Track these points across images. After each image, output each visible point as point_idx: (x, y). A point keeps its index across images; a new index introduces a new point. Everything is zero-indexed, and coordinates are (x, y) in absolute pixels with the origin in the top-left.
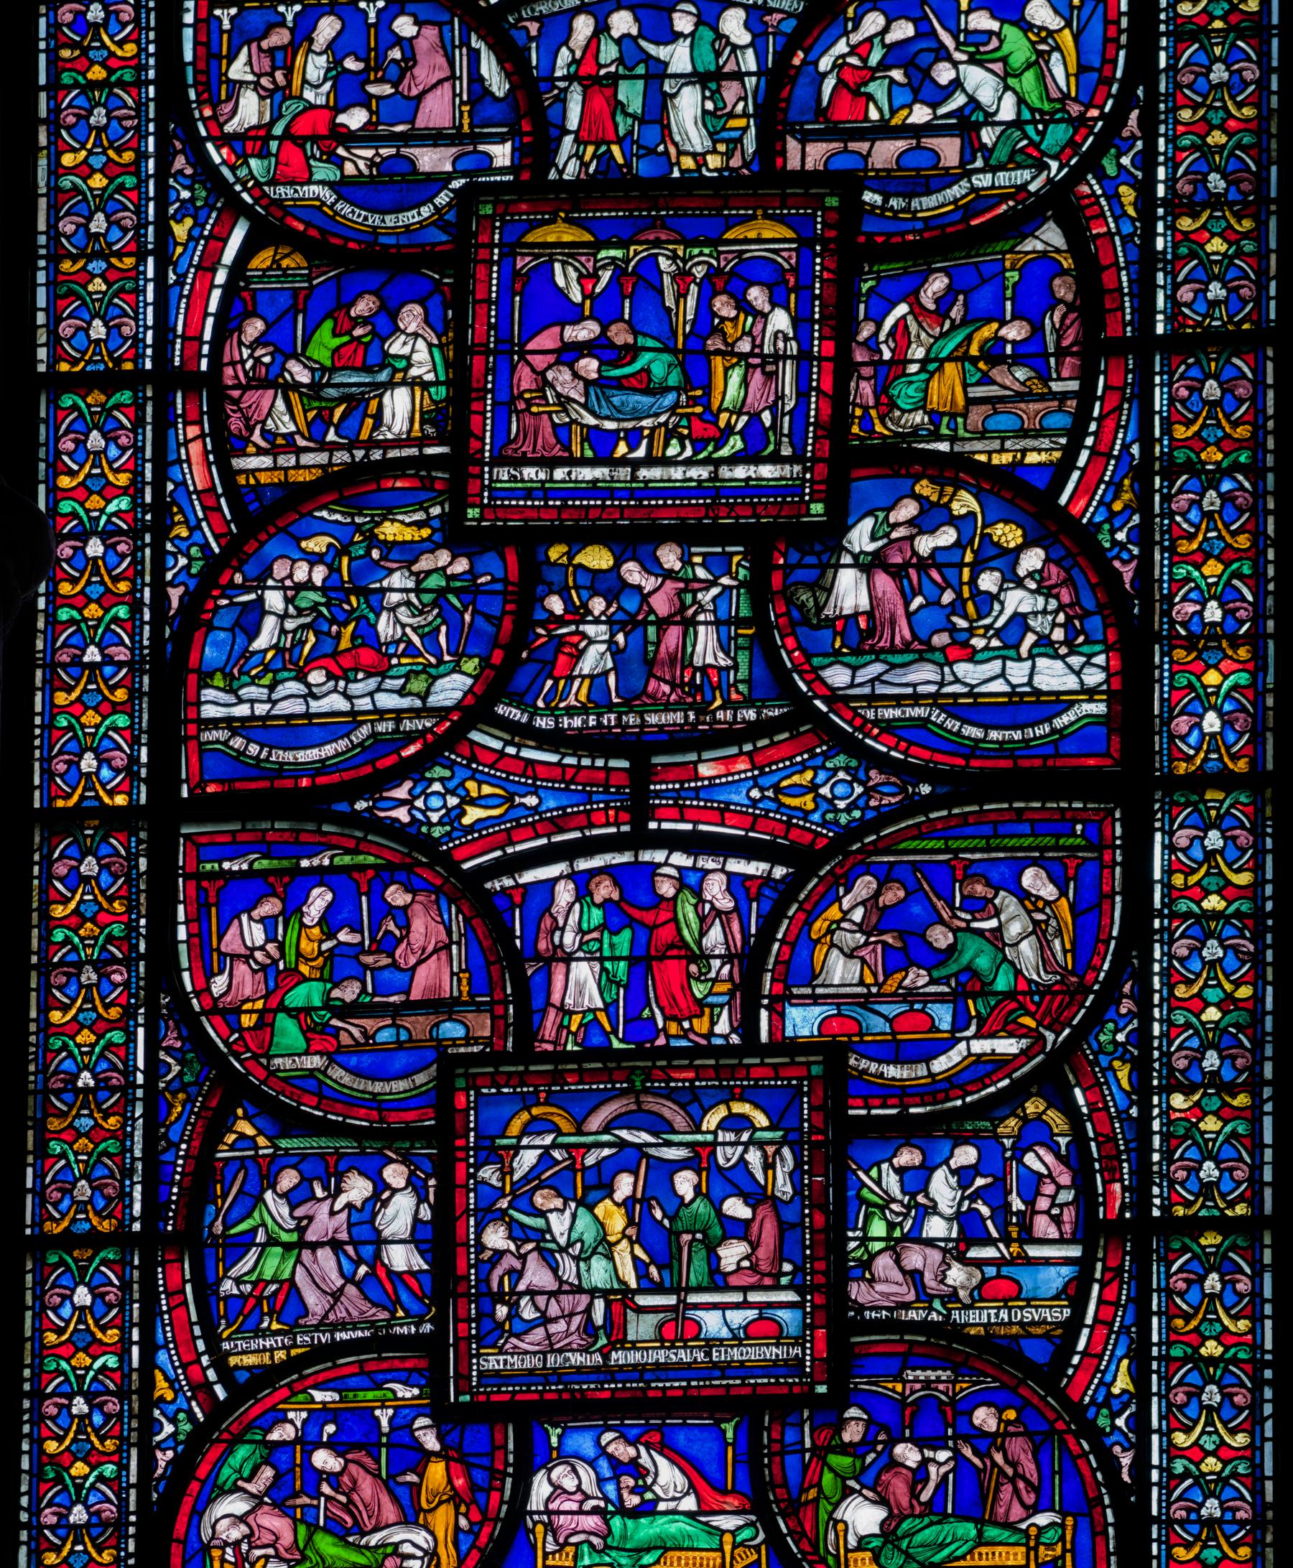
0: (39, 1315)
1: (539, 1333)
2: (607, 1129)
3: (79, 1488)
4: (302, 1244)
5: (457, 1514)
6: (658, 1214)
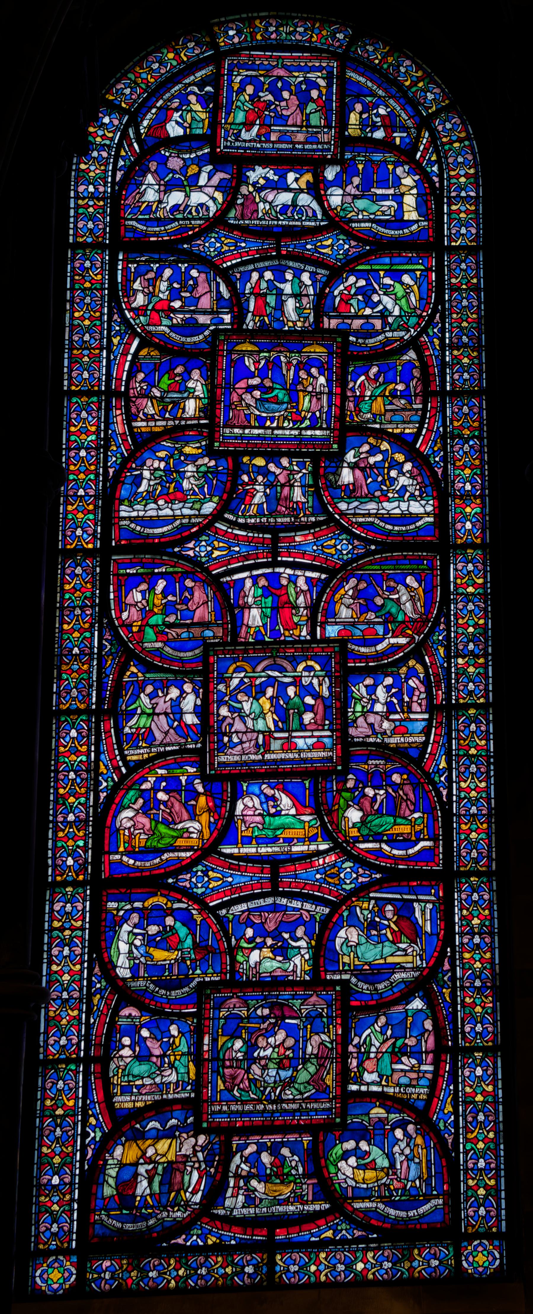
0: (58, 741)
1: (239, 747)
2: (263, 671)
3: (71, 807)
4: (154, 714)
6: (282, 703)
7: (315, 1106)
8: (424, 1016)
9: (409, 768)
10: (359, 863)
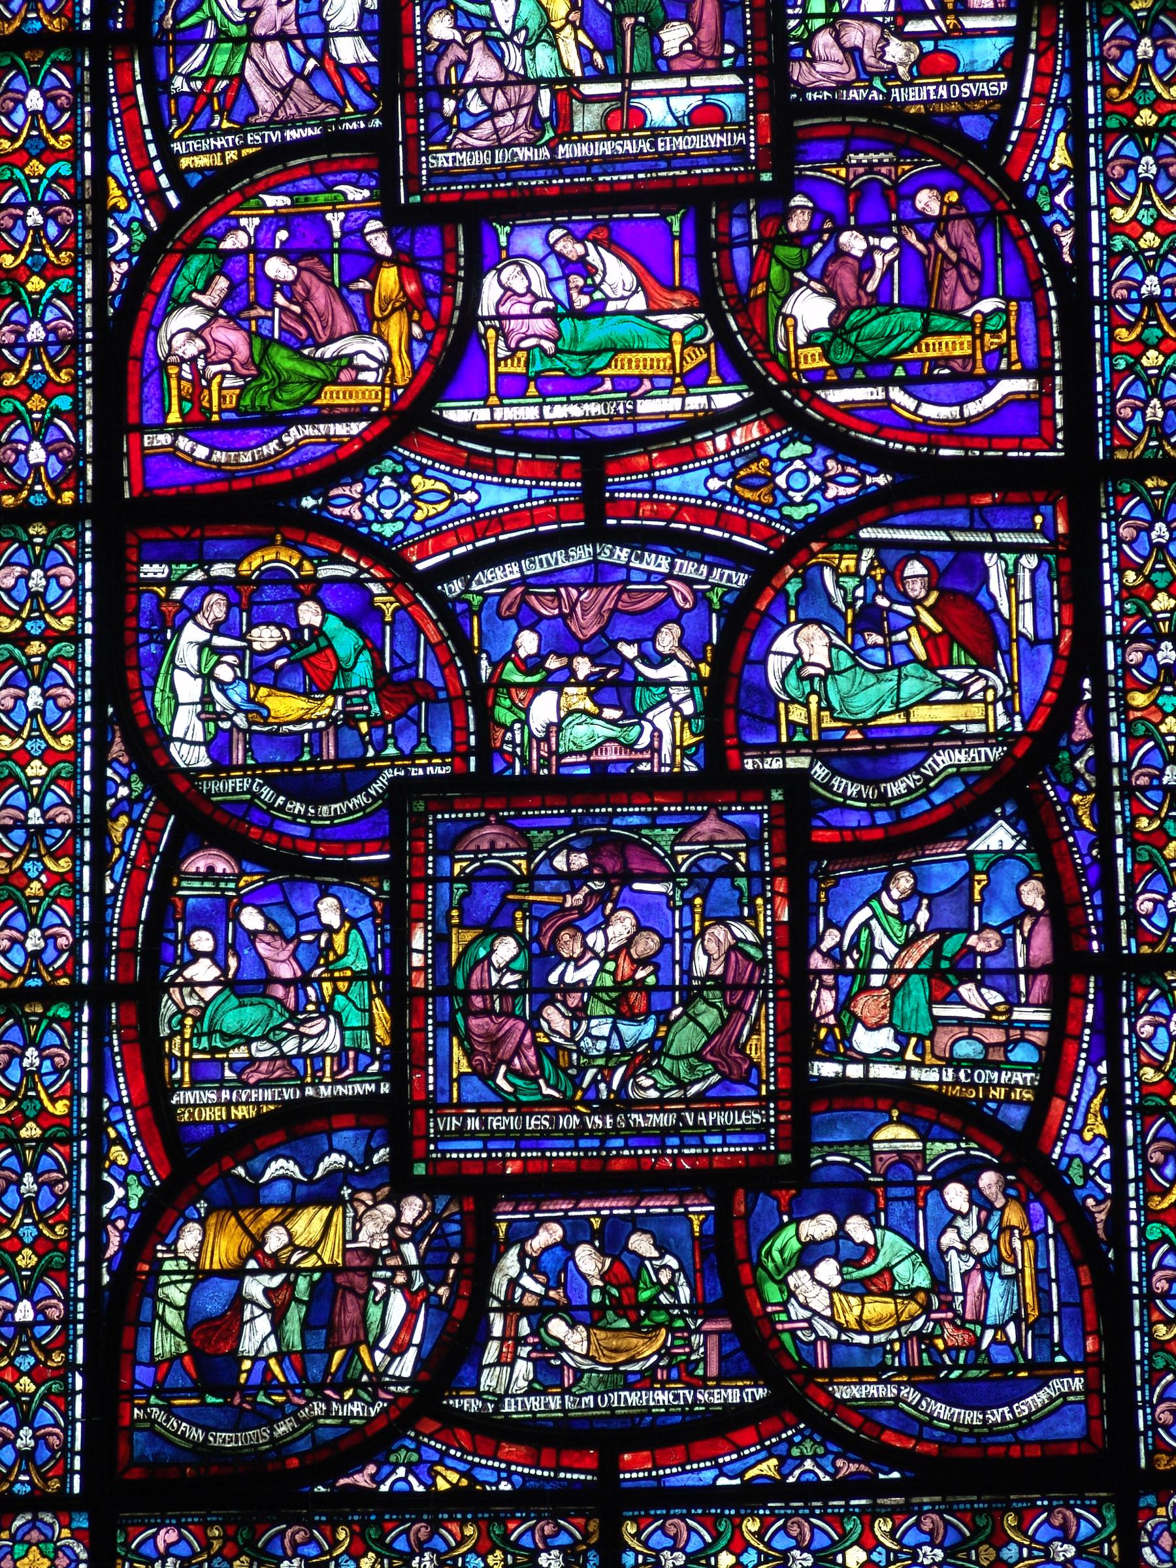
1: (487, 127)
3: (35, 304)
4: (251, 38)
5: (410, 321)
7: (722, 1118)
8: (1019, 872)
9: (965, 172)
10: (826, 445)
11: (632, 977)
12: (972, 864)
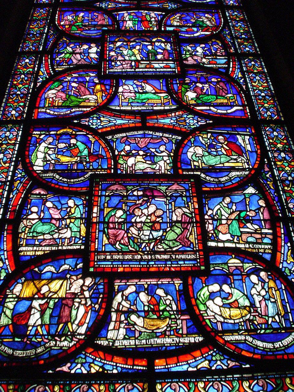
7: (183, 257)
11: (156, 220)
12: (245, 196)
